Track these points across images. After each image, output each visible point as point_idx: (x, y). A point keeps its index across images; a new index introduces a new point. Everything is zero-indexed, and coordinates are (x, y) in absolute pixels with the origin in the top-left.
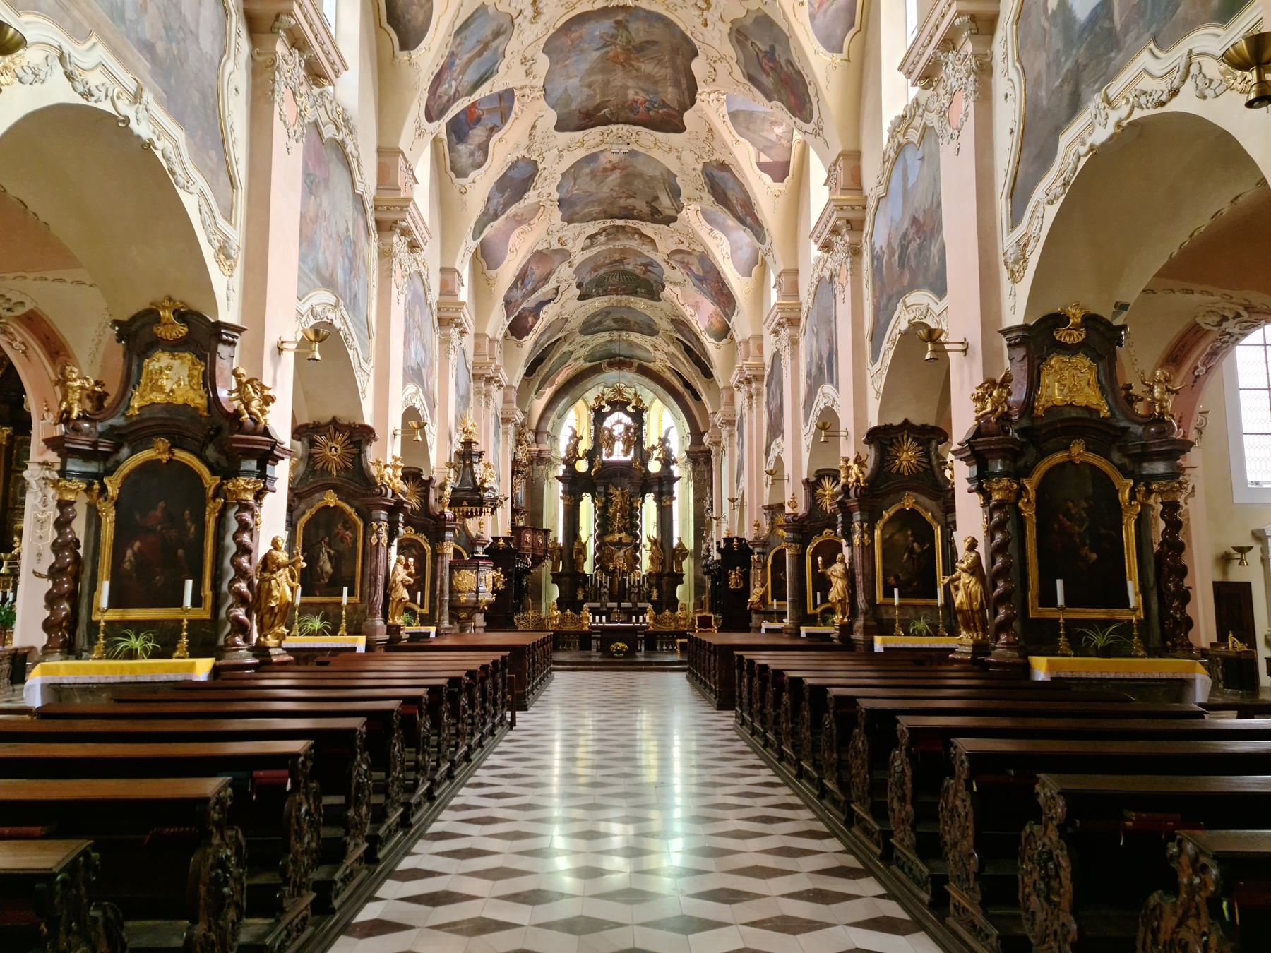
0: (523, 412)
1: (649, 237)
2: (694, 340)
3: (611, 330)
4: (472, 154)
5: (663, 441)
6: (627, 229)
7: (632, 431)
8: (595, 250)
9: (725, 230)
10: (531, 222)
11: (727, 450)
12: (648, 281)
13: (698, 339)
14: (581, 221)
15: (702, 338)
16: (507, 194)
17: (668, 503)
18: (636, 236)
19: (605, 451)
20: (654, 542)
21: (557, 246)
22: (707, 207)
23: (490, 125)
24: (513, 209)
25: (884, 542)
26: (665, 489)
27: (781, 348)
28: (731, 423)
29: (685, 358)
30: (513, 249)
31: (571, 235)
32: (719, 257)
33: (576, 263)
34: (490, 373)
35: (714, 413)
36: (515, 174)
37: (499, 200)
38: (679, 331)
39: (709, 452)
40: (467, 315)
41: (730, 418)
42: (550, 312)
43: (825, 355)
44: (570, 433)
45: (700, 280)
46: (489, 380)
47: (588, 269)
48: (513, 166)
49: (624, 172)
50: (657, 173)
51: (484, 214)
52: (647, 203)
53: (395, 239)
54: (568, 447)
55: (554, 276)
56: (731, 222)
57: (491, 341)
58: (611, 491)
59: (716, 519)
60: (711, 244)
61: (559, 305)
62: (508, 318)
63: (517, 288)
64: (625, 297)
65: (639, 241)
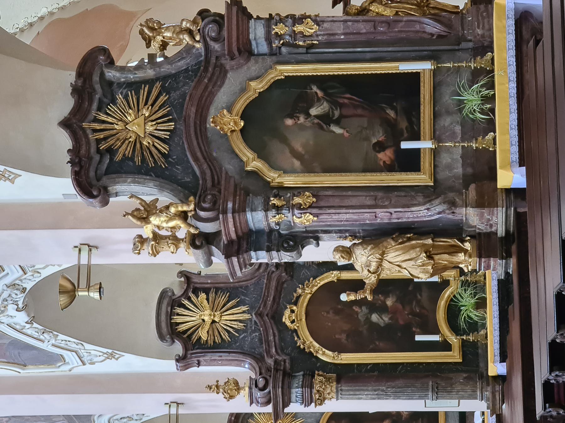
25: (308, 169)
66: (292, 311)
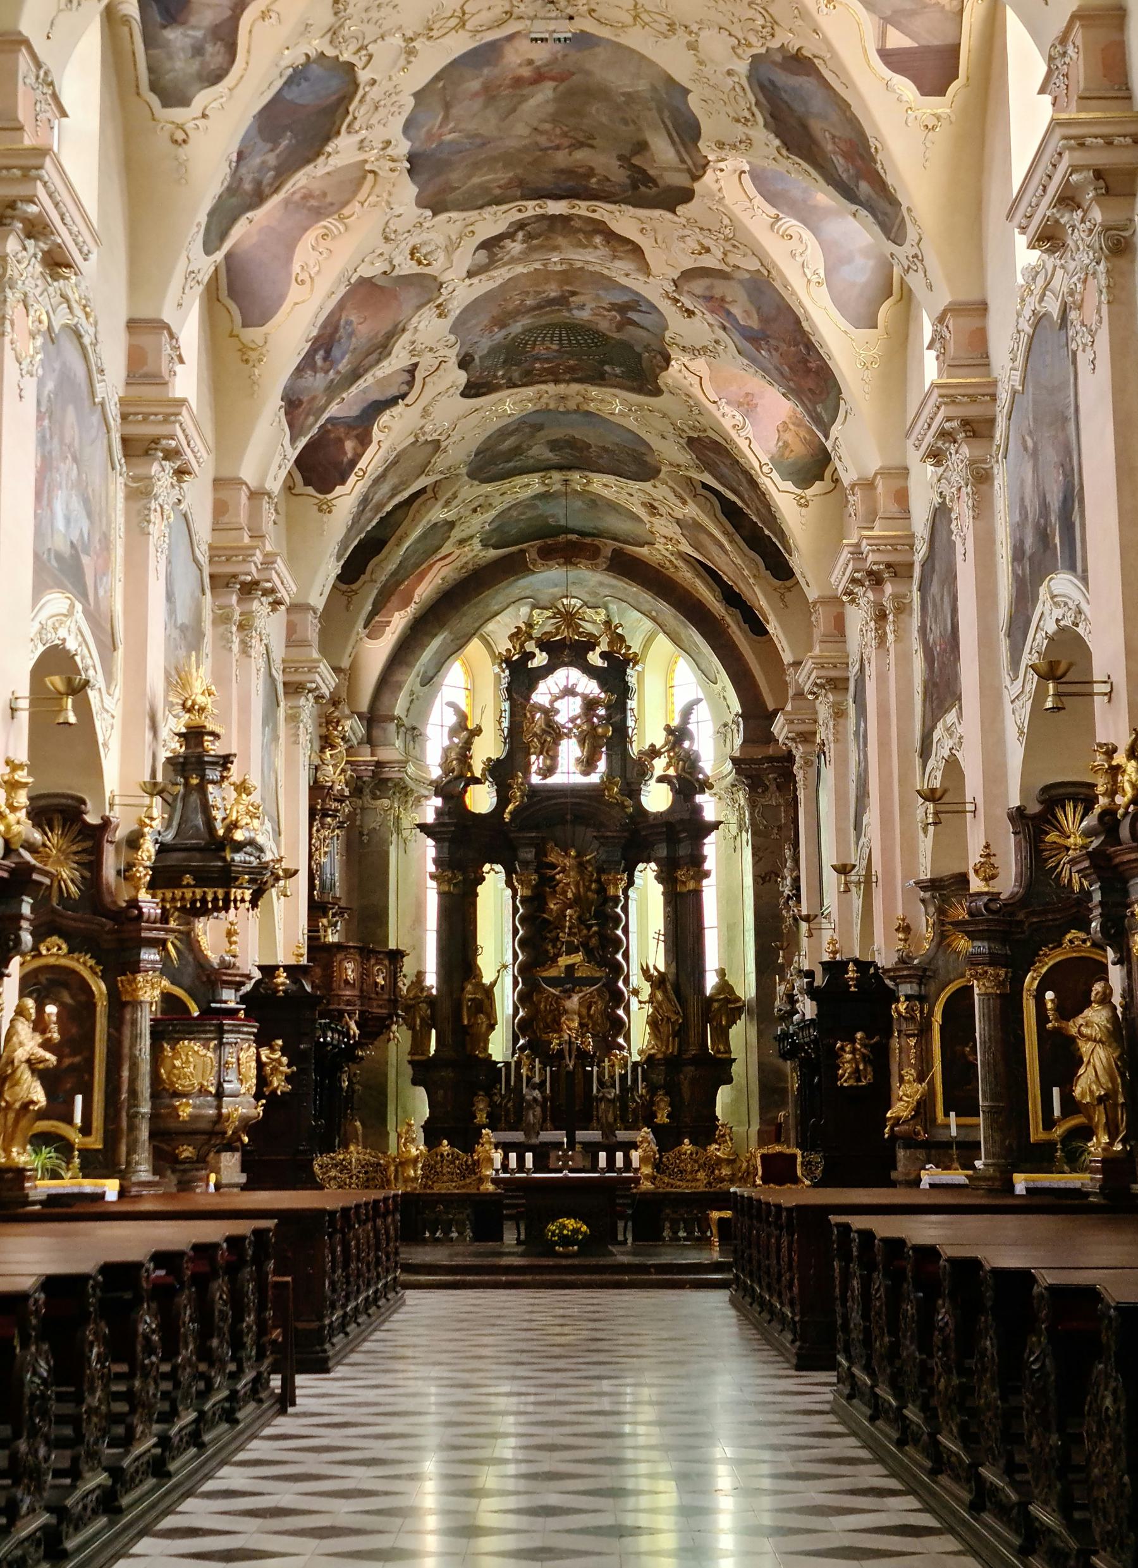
0: (337, 670)
1: (628, 241)
2: (744, 488)
3: (544, 468)
4: (198, 50)
5: (678, 735)
6: (577, 224)
7: (602, 712)
8: (501, 275)
9: (809, 217)
10: (346, 211)
11: (831, 749)
13: (754, 484)
14: (462, 207)
15: (765, 483)
16: (285, 143)
18: (598, 240)
19: (536, 762)
20: (658, 982)
21: (408, 267)
24: (302, 180)
26: (683, 851)
28: (837, 684)
29: (725, 533)
30: (304, 276)
31: (441, 240)
32: (797, 283)
33: (455, 308)
34: (252, 571)
35: (797, 664)
36: (305, 96)
37: (266, 157)
38: (709, 467)
40: (191, 430)
42: (397, 425)
45: (754, 339)
46: (249, 589)
47: (484, 319)
48: (298, 76)
49: (562, 87)
50: (642, 86)
51: (232, 190)
52: (620, 158)
53: (12, 245)
55: (405, 338)
56: (824, 197)
57: (256, 495)
58: (552, 858)
59: (807, 919)
60: (775, 249)
61: (418, 408)
62: (293, 440)
63: (314, 368)
64: (575, 387)
65: (604, 251)
66: (1084, 941)
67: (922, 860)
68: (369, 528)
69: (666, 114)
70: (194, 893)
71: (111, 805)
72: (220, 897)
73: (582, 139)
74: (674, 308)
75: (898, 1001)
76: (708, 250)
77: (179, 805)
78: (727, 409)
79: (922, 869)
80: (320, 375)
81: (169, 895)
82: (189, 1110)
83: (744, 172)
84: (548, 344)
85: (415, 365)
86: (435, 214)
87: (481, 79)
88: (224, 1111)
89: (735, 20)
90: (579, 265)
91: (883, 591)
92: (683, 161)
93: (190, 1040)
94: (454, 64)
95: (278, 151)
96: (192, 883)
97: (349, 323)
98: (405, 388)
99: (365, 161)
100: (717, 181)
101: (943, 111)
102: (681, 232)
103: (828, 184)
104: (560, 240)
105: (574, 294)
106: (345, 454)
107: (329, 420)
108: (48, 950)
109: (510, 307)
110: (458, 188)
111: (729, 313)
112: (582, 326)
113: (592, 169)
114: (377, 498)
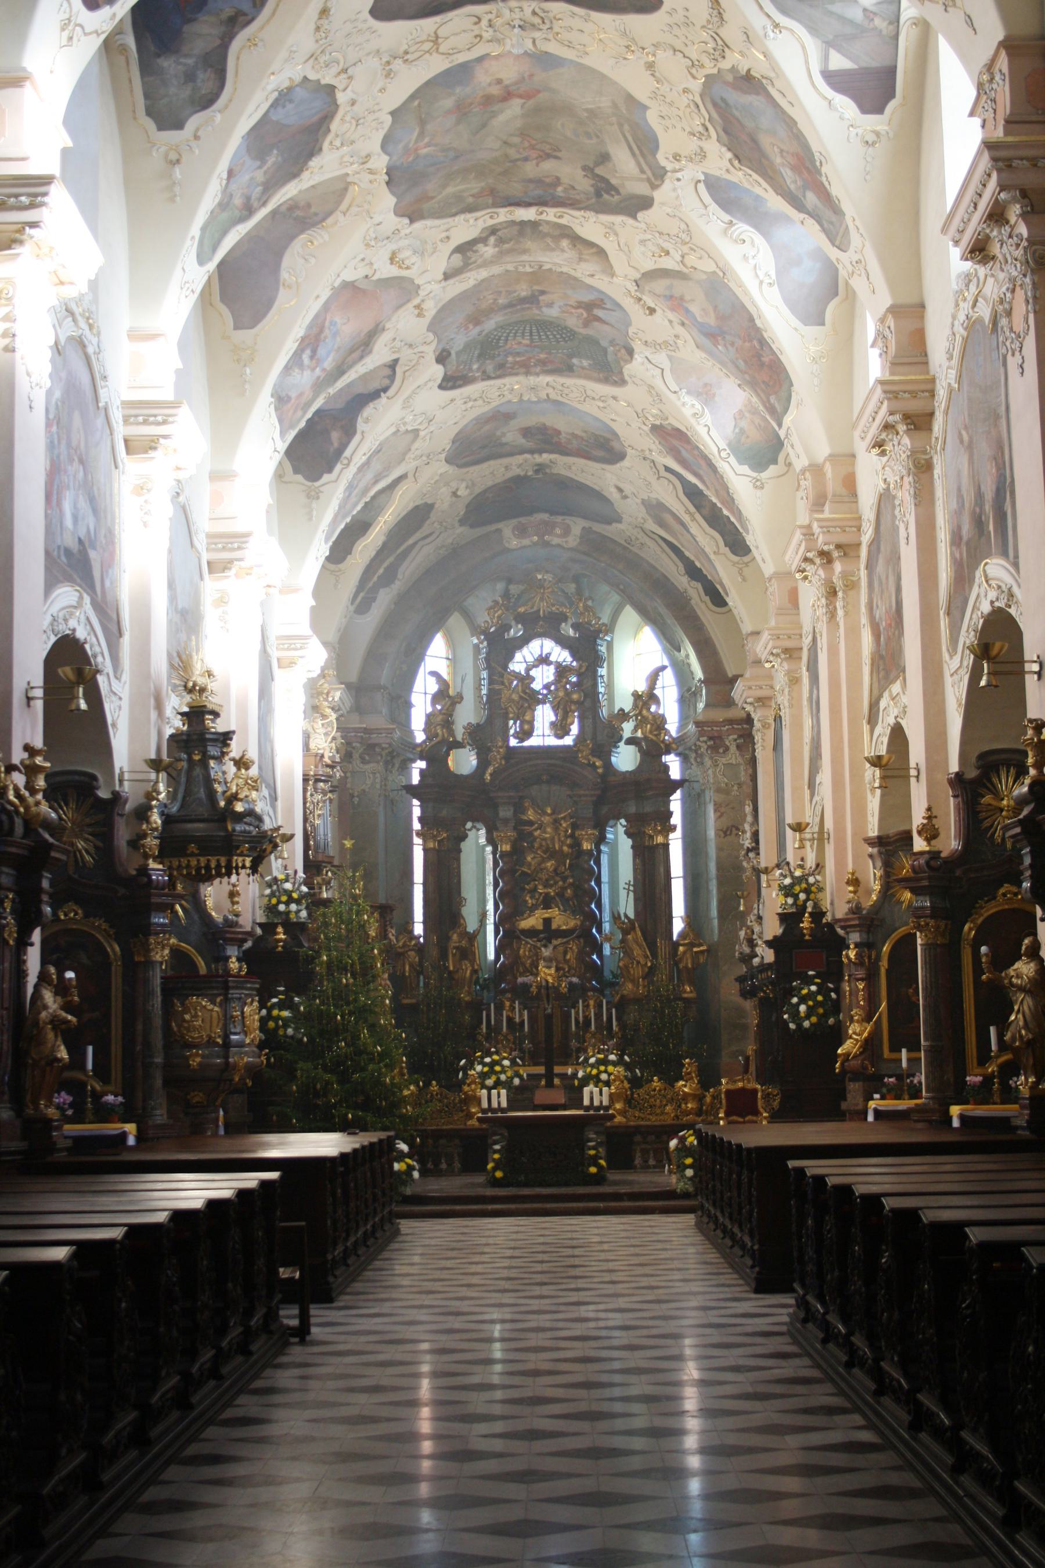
6: (544, 228)
12: (597, 343)
14: (440, 213)
15: (723, 467)
16: (271, 160)
17: (660, 839)
18: (565, 243)
21: (386, 270)
22: (718, 173)
23: (228, 12)
27: (892, 479)
33: (431, 308)
36: (290, 116)
39: (749, 720)
41: (789, 644)
43: (989, 494)
44: (433, 687)
45: (712, 335)
50: (605, 103)
52: (584, 168)
54: (429, 717)
61: (399, 402)
62: (283, 434)
63: (301, 366)
65: (570, 254)
67: (870, 819)
68: (355, 512)
69: (626, 127)
70: (198, 861)
71: (121, 781)
72: (223, 864)
73: (548, 151)
74: (637, 306)
75: (848, 948)
76: (668, 253)
77: (183, 779)
78: (689, 400)
79: (870, 826)
80: (307, 373)
81: (175, 863)
82: (198, 1060)
83: (699, 181)
84: (519, 339)
85: (396, 361)
86: (412, 221)
87: (453, 98)
88: (231, 1060)
89: (689, 43)
90: (546, 267)
91: (833, 570)
92: (642, 171)
93: (198, 996)
94: (428, 84)
95: (265, 168)
96: (196, 852)
97: (333, 323)
98: (387, 382)
99: (347, 175)
100: (675, 190)
101: (882, 128)
102: (643, 237)
103: (777, 194)
104: (529, 244)
105: (543, 293)
106: (332, 444)
107: (318, 413)
108: (66, 915)
109: (484, 305)
110: (433, 198)
111: (687, 311)
112: (551, 323)
113: (558, 179)
114: (362, 485)
